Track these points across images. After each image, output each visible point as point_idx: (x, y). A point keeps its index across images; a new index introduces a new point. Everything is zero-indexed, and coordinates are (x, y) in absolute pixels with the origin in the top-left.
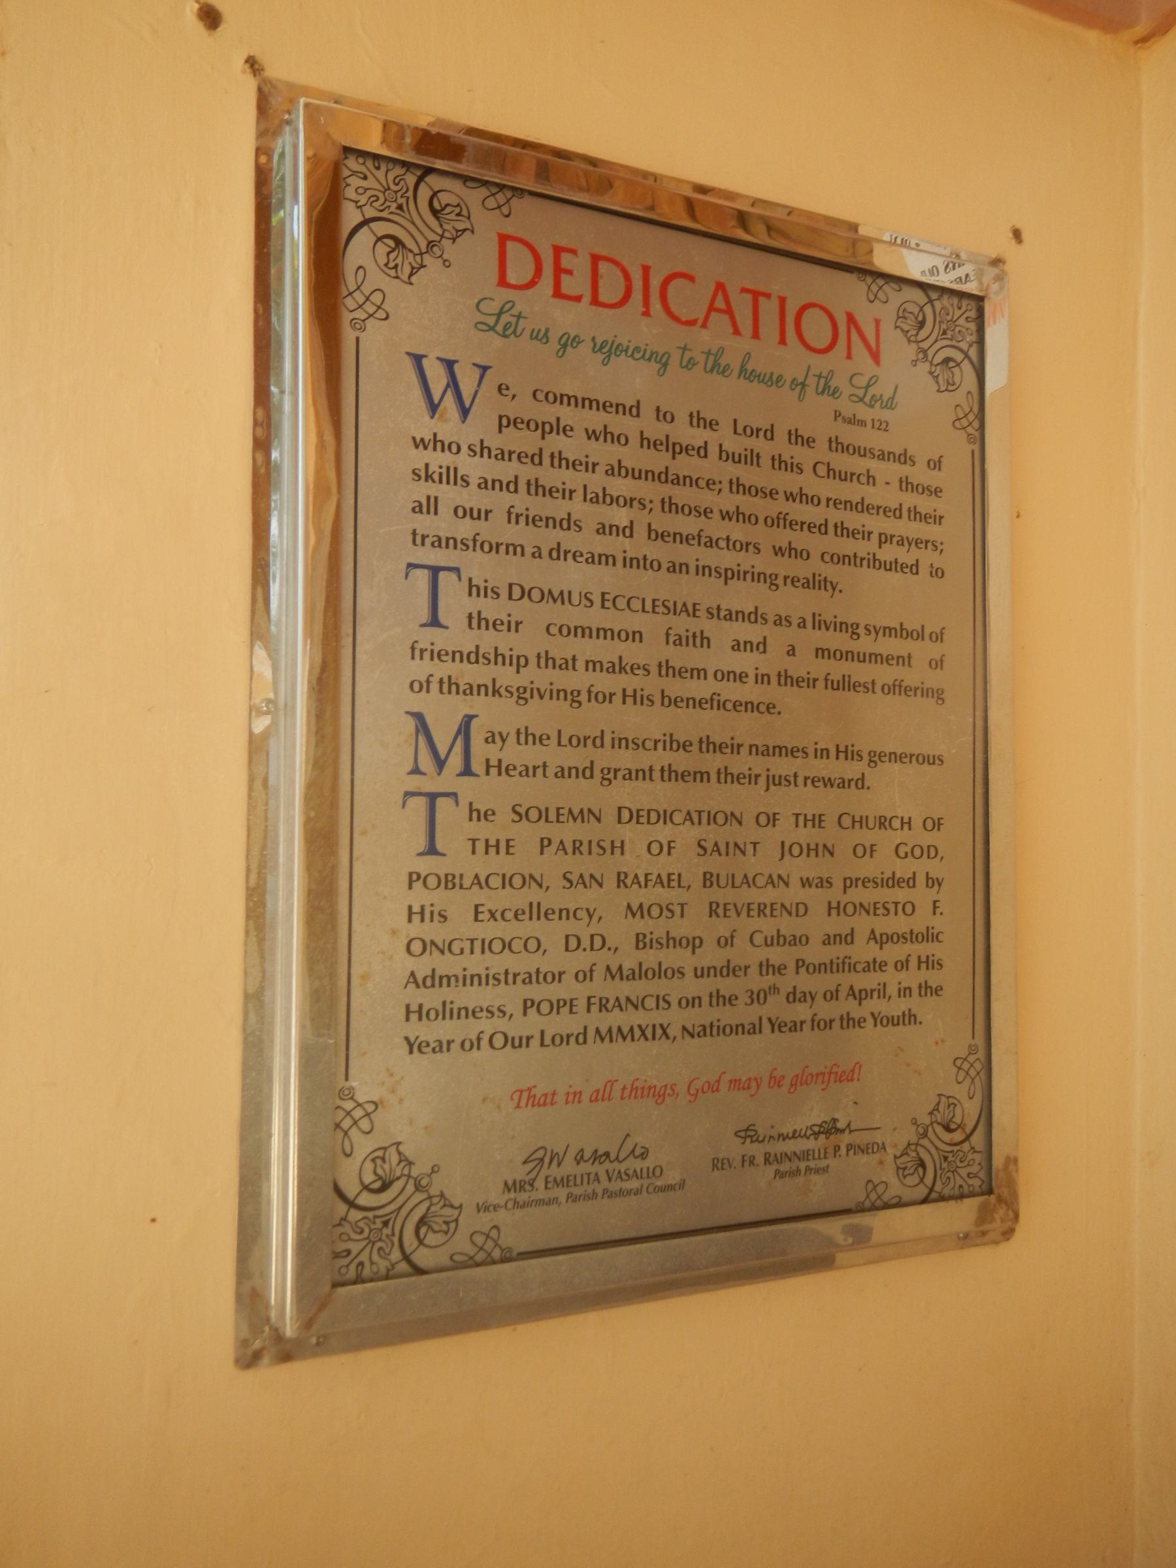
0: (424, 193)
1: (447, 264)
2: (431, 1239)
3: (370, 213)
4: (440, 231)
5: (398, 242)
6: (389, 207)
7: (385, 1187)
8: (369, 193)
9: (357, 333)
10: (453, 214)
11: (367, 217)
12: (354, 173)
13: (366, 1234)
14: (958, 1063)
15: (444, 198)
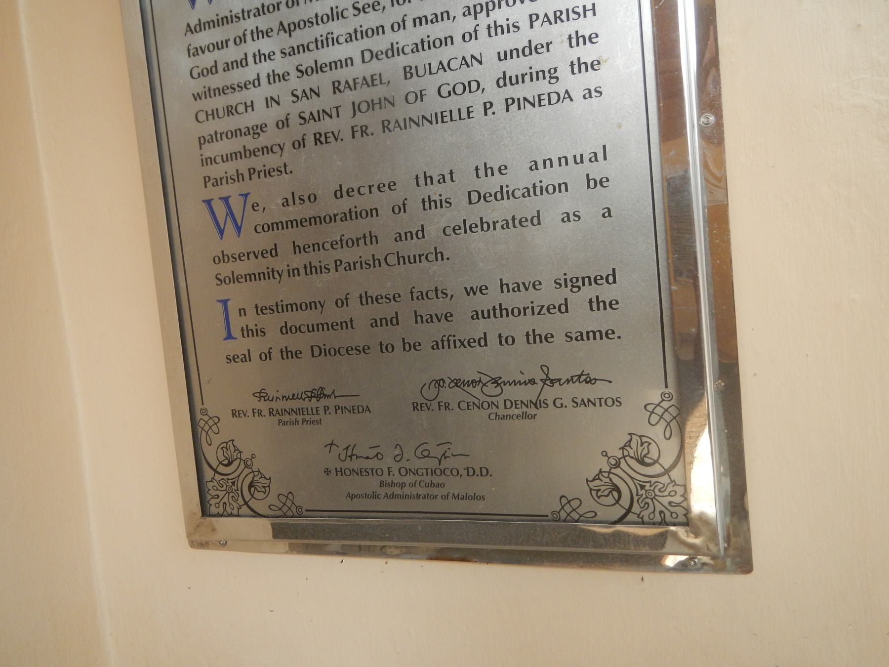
0: (625, 501)
1: (605, 454)
3: (665, 480)
4: (611, 476)
5: (641, 462)
6: (651, 486)
8: (666, 493)
9: (667, 391)
10: (602, 490)
11: (667, 476)
12: (678, 505)
15: (610, 500)
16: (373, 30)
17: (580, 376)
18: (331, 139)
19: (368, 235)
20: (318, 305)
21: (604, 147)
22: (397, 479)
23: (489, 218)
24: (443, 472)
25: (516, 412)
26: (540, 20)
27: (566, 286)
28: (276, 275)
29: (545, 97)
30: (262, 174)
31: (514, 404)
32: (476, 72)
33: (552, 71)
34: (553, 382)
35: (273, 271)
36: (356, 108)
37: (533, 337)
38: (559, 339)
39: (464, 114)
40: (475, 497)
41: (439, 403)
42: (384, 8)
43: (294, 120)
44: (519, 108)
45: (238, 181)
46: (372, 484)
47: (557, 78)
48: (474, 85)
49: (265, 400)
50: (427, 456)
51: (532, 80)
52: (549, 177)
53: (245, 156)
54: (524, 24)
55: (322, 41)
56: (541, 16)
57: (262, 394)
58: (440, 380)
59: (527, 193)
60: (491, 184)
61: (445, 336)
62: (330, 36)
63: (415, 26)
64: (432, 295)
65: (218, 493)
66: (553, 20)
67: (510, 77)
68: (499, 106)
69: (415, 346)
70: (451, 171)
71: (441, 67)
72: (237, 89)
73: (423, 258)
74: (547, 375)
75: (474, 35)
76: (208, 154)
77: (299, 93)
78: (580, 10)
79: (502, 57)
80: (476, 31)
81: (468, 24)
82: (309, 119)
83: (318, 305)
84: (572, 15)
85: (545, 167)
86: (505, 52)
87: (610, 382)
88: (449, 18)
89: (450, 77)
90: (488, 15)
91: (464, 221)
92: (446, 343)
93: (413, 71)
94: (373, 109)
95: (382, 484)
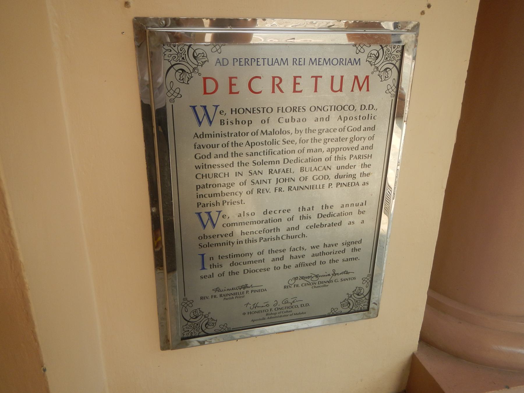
2: (375, 52)
7: (386, 69)
13: (392, 56)
14: (179, 96)
16: (290, 151)
17: (344, 272)
18: (265, 192)
19: (276, 228)
20: (250, 254)
21: (366, 201)
22: (274, 312)
23: (324, 223)
24: (292, 307)
25: (322, 285)
26: (353, 157)
27: (346, 245)
28: (231, 244)
29: (351, 184)
30: (229, 203)
31: (322, 282)
32: (328, 172)
33: (354, 175)
34: (335, 274)
35: (230, 242)
36: (278, 181)
37: (332, 261)
38: (340, 261)
39: (321, 187)
40: (303, 313)
41: (294, 285)
42: (296, 143)
43: (249, 183)
44: (341, 187)
45: (217, 205)
46: (264, 315)
47: (355, 178)
48: (326, 177)
49: (218, 291)
50: (287, 303)
51: (347, 177)
52: (347, 210)
53: (222, 196)
54: (348, 158)
55: (267, 152)
56: (354, 156)
57: (217, 290)
58: (296, 277)
59: (339, 215)
60: (326, 212)
61: (301, 263)
62: (270, 151)
63: (308, 152)
64: (298, 249)
65: (189, 329)
66: (357, 158)
67: (340, 176)
68: (334, 185)
69: (289, 267)
70: (313, 206)
71: (315, 169)
72: (220, 165)
73: (297, 237)
74: (334, 273)
75: (330, 159)
76: (201, 193)
77: (253, 172)
78: (367, 156)
79: (338, 168)
80: (330, 158)
81: (328, 155)
82: (256, 183)
83: (250, 254)
84: (364, 157)
85: (346, 207)
86: (340, 167)
87: (354, 273)
88: (321, 151)
89: (318, 173)
90: (336, 153)
91: (315, 224)
92: (301, 265)
93: (304, 169)
94: (285, 182)
95: (267, 315)
